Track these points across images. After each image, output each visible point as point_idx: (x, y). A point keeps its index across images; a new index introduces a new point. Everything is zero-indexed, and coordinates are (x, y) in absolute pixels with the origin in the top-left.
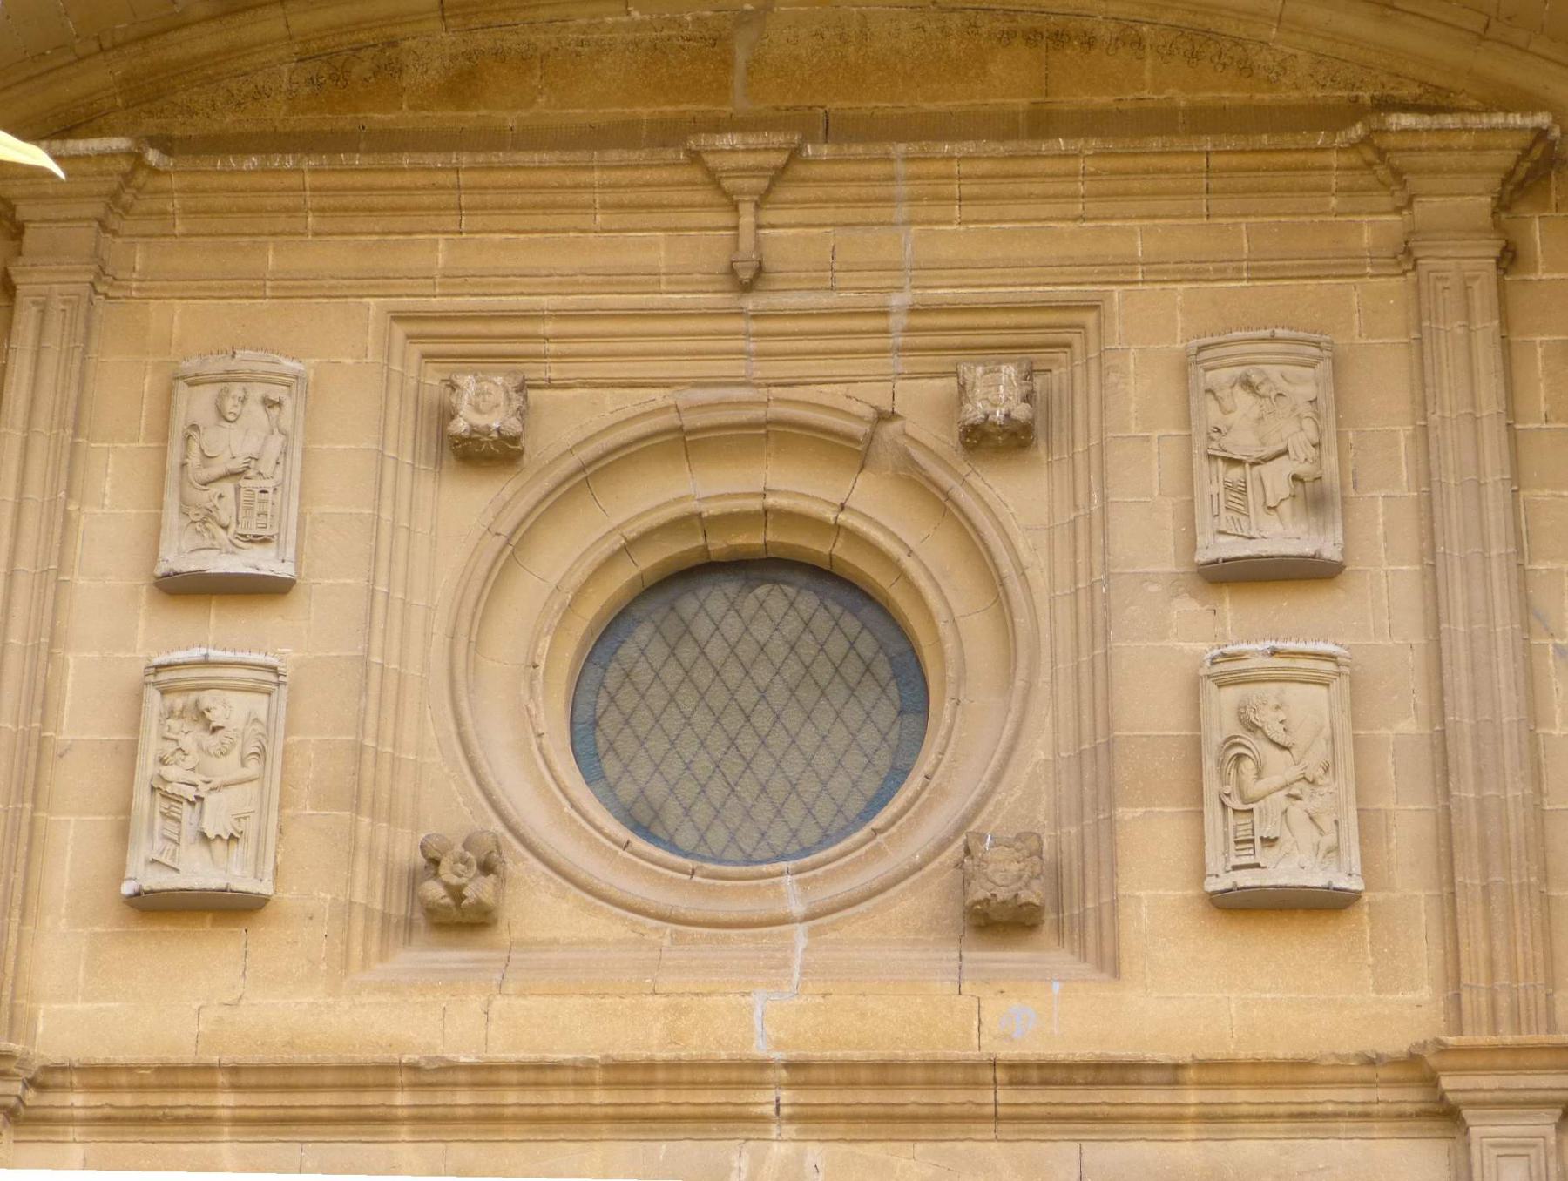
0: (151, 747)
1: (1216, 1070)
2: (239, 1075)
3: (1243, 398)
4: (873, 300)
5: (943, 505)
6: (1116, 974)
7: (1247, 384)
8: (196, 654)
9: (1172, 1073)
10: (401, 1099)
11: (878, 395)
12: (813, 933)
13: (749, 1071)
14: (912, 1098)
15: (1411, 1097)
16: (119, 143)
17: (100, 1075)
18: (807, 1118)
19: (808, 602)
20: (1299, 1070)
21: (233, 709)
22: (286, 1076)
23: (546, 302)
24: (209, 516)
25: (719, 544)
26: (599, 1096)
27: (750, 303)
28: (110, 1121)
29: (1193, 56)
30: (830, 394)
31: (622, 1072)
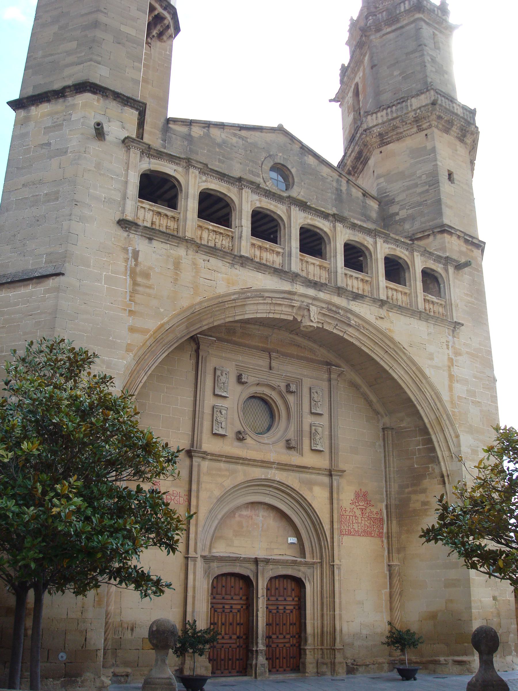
0: (215, 415)
1: (313, 468)
2: (226, 457)
3: (316, 394)
4: (282, 374)
5: (283, 397)
6: (302, 456)
7: (317, 393)
8: (221, 405)
9: (309, 468)
10: (241, 461)
11: (278, 384)
12: (273, 446)
13: (273, 463)
14: (286, 468)
15: (328, 473)
16: (215, 339)
17: (212, 455)
18: (277, 468)
19: (261, 403)
20: (320, 469)
21: (224, 412)
22: (231, 457)
23: (251, 367)
24: (221, 388)
25: (256, 395)
26: (259, 464)
27: (271, 371)
28: (211, 460)
29: (310, 352)
30: (273, 382)
31: (263, 462)
